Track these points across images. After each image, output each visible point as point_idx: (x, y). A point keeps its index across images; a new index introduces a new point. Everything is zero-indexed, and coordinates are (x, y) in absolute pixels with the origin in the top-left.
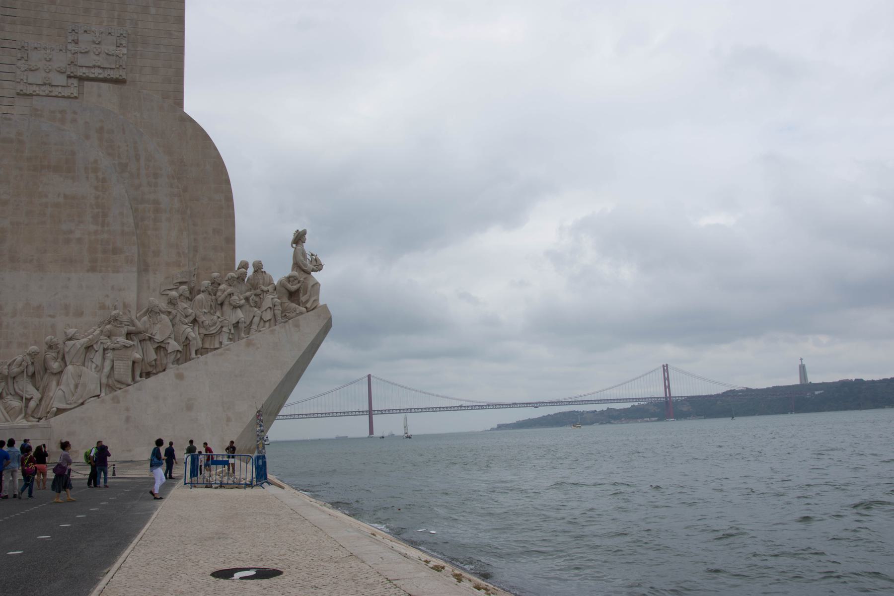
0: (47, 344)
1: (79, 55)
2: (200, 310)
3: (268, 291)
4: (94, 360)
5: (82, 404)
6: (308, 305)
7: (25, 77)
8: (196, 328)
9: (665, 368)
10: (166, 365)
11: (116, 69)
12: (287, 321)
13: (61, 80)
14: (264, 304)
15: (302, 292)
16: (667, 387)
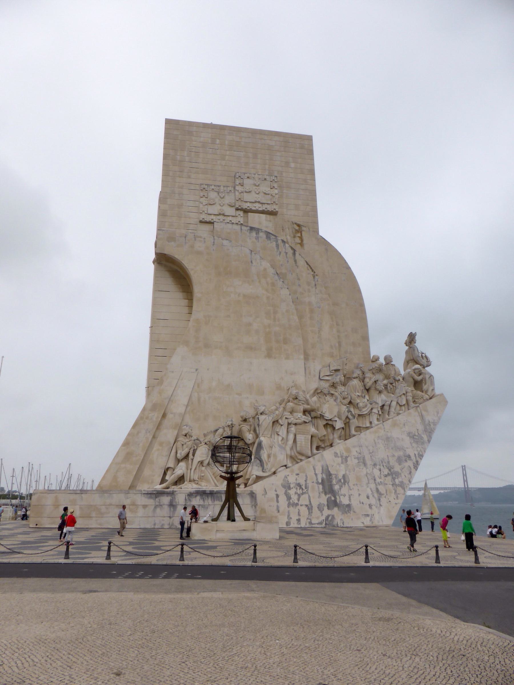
0: (242, 417)
1: (245, 194)
2: (355, 393)
3: (399, 380)
4: (280, 433)
5: (274, 473)
6: (429, 393)
7: (206, 210)
8: (352, 409)
9: (464, 468)
10: (333, 439)
11: (271, 205)
12: (418, 406)
13: (231, 211)
14: (397, 391)
15: (424, 382)
16: (465, 481)
